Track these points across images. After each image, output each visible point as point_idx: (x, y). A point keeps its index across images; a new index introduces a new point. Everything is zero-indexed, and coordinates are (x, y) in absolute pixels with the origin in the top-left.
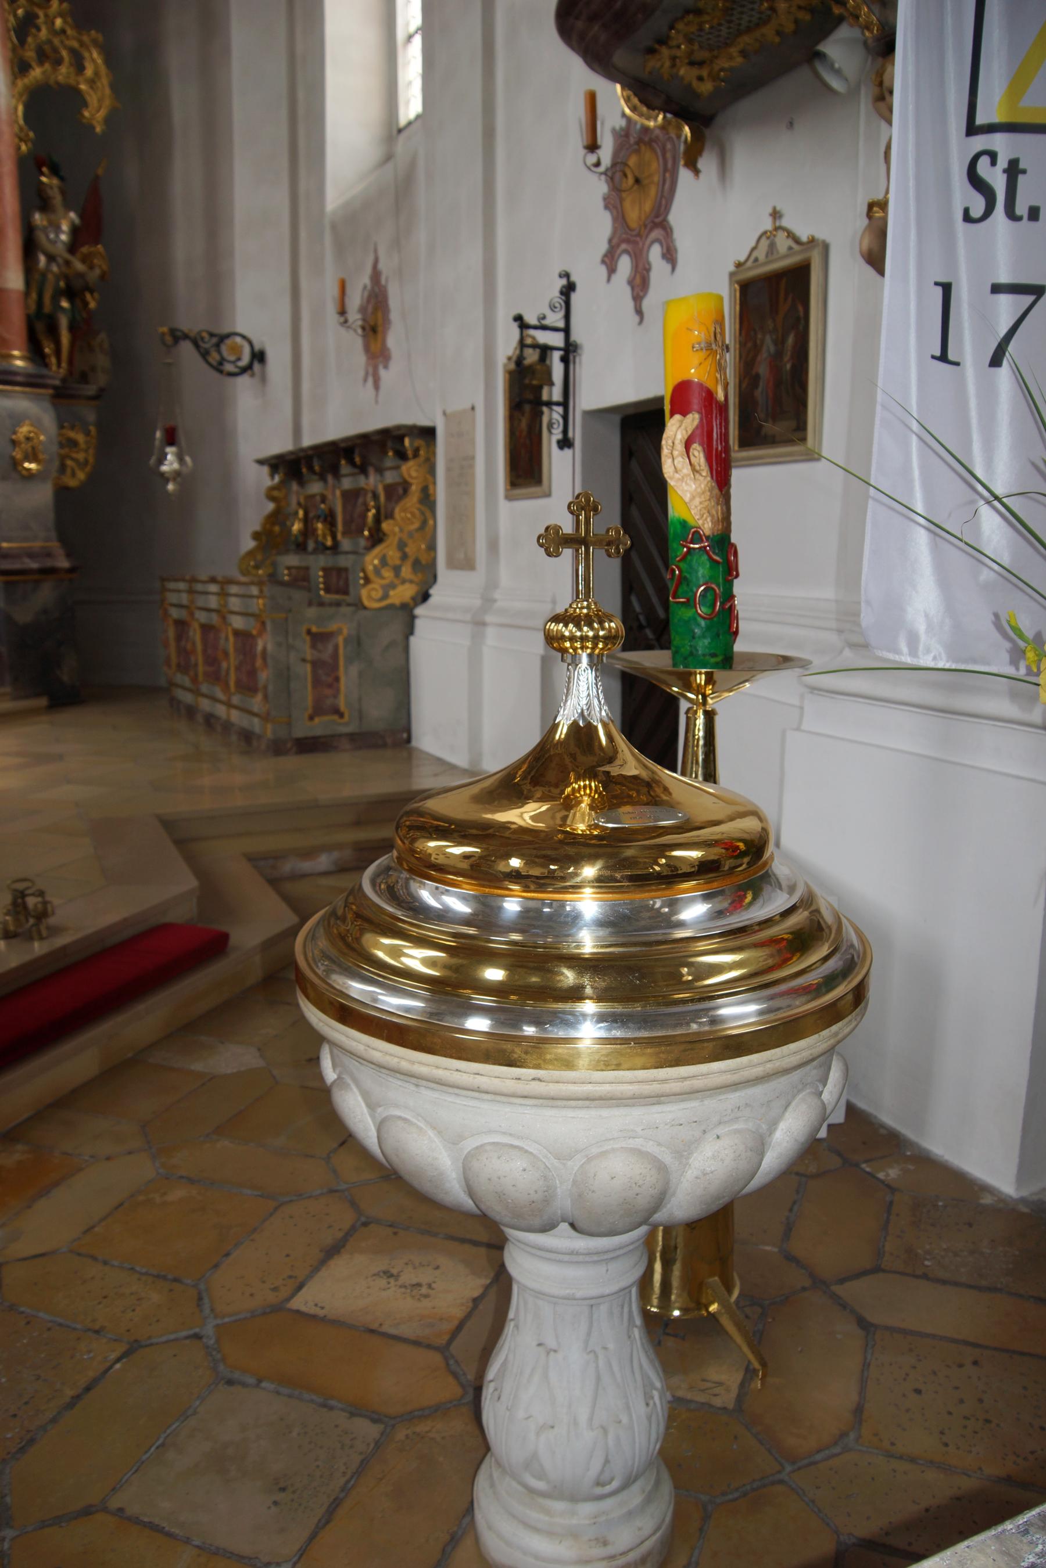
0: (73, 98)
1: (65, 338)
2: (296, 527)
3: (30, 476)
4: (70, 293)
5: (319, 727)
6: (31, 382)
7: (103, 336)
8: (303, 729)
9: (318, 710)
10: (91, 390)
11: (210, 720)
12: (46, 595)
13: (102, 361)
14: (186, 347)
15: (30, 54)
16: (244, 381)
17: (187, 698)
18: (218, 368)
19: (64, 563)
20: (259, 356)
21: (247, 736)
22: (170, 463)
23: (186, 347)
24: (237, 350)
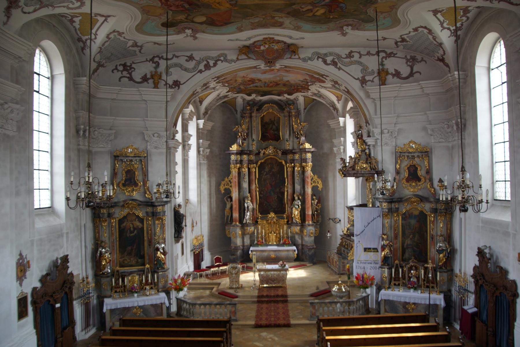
0: (318, 187)
1: (316, 216)
2: (344, 244)
3: (311, 236)
4: (316, 211)
5: (343, 272)
6: (312, 225)
7: (320, 216)
8: (341, 272)
9: (343, 270)
10: (319, 224)
11: (332, 269)
12: (313, 251)
13: (320, 219)
14: (331, 220)
15: (312, 183)
16: (338, 224)
17: (330, 265)
18: (335, 223)
19: (315, 247)
20: (340, 221)
21: (336, 272)
22: (329, 235)
23: (331, 220)
24: (337, 220)
